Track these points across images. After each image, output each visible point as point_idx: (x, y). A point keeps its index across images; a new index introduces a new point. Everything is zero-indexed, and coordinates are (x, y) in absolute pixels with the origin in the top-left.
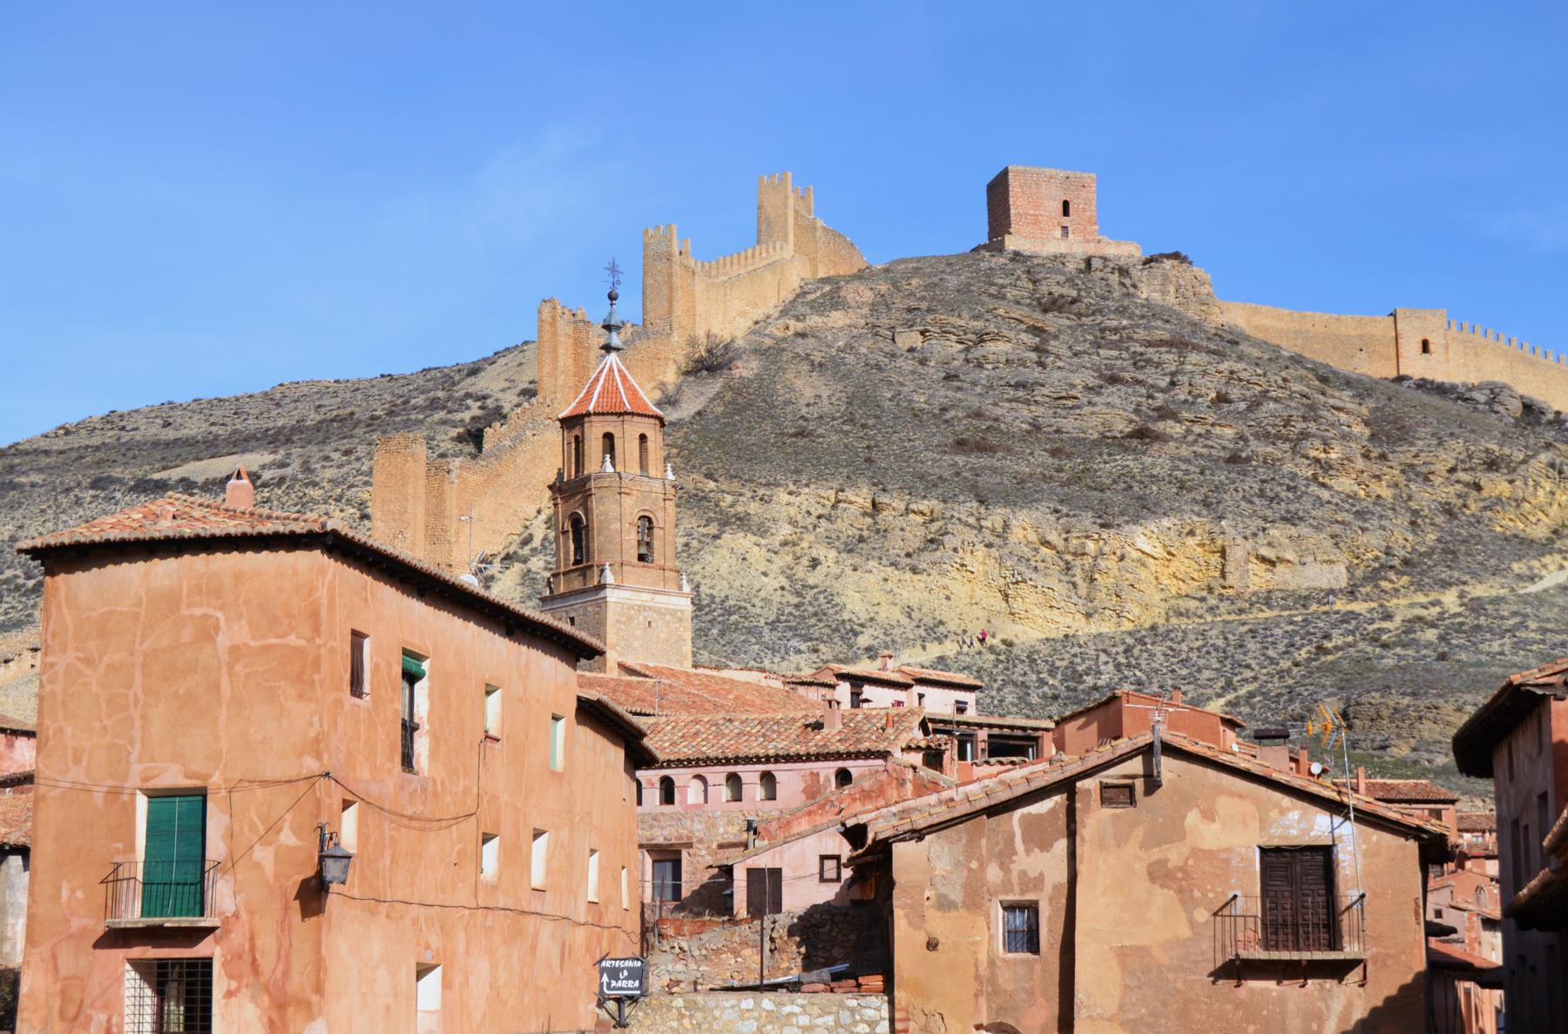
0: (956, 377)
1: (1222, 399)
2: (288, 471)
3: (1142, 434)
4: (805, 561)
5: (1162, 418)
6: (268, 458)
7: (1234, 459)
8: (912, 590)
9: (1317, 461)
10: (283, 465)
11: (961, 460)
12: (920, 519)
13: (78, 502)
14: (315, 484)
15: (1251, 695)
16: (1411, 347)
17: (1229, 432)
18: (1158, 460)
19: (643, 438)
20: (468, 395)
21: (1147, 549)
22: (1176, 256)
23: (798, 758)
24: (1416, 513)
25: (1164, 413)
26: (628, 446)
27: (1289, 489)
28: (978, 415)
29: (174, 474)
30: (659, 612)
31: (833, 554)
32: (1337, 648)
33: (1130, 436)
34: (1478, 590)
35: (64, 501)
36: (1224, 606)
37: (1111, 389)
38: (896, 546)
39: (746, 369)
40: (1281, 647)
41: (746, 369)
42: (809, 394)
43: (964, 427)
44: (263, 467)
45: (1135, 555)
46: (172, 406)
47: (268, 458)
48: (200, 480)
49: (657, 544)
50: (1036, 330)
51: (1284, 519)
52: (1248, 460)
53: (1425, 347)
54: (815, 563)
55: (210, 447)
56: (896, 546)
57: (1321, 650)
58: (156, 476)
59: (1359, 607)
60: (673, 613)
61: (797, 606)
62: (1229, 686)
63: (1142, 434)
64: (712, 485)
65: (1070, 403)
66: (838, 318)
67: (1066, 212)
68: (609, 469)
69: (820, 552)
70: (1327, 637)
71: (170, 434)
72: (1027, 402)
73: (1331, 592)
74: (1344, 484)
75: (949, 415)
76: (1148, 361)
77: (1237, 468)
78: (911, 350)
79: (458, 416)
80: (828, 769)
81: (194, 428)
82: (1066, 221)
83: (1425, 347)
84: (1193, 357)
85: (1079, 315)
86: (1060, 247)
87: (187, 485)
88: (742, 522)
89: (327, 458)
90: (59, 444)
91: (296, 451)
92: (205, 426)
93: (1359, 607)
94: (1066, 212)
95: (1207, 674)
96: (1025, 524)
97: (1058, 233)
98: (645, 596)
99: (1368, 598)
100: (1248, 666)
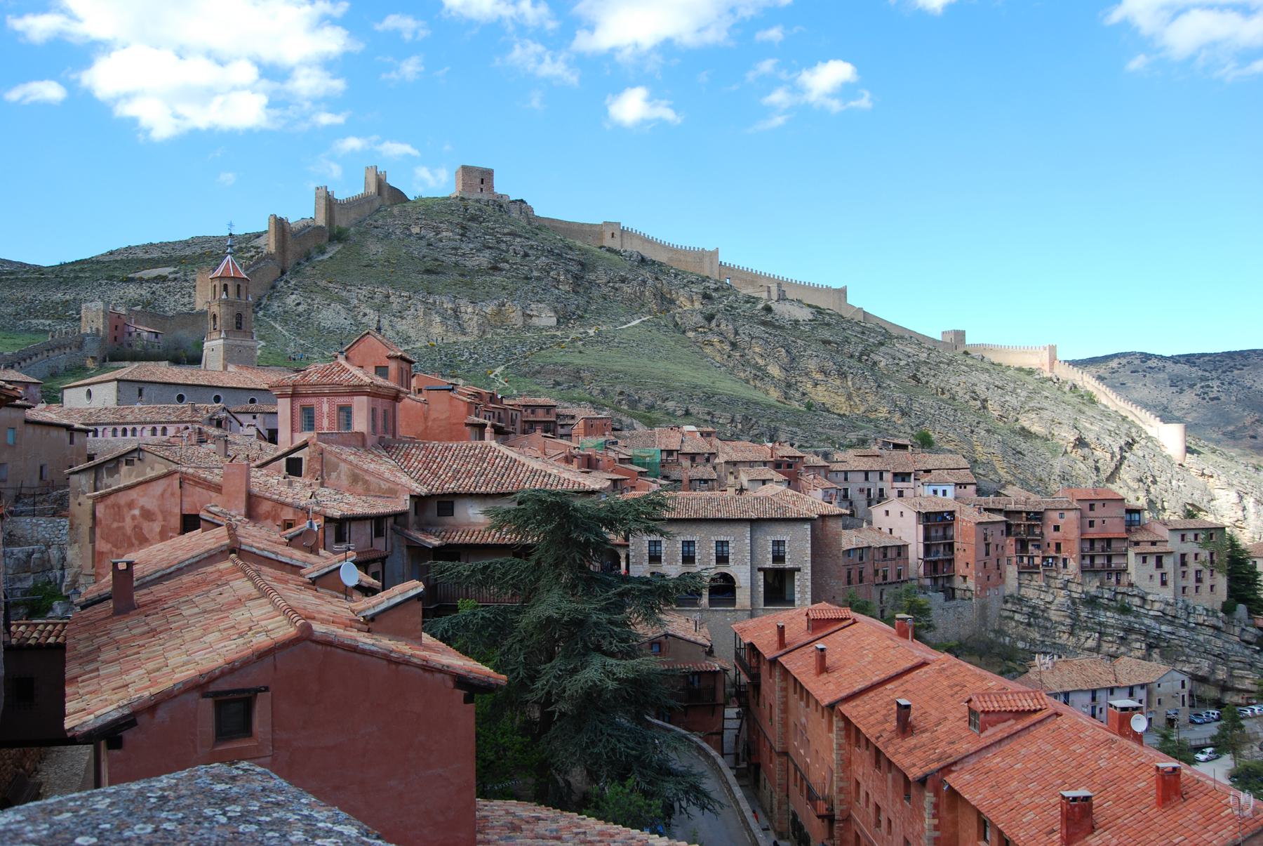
0: (431, 245)
1: (526, 255)
2: (178, 275)
3: (495, 268)
4: (361, 313)
5: (504, 262)
6: (172, 269)
7: (526, 278)
9: (556, 279)
10: (177, 273)
11: (425, 277)
12: (405, 299)
13: (100, 285)
14: (186, 281)
15: (513, 365)
16: (608, 236)
17: (526, 268)
18: (498, 279)
19: (239, 286)
20: (252, 247)
21: (487, 311)
22: (522, 201)
23: (172, 422)
24: (591, 298)
26: (231, 289)
27: (543, 290)
28: (436, 260)
29: (138, 275)
30: (245, 347)
31: (372, 311)
32: (547, 348)
33: (491, 269)
34: (604, 328)
35: (95, 284)
36: (513, 332)
37: (487, 251)
38: (395, 307)
40: (528, 347)
42: (374, 251)
43: (429, 264)
44: (170, 273)
45: (482, 313)
46: (151, 244)
47: (172, 269)
48: (146, 278)
49: (243, 323)
50: (463, 228)
51: (537, 301)
52: (531, 278)
54: (365, 315)
55: (155, 263)
56: (395, 307)
57: (541, 348)
58: (130, 276)
59: (559, 333)
60: (249, 347)
61: (355, 331)
62: (508, 361)
64: (331, 285)
65: (471, 256)
67: (482, 183)
68: (224, 296)
69: (368, 311)
70: (545, 344)
71: (147, 256)
72: (455, 255)
73: (551, 327)
75: (425, 259)
76: (502, 241)
77: (525, 281)
78: (417, 234)
79: (245, 255)
80: (182, 426)
81: (156, 254)
82: (482, 186)
83: (613, 234)
84: (518, 240)
85: (481, 223)
86: (480, 196)
87: (141, 280)
89: (193, 271)
90: (107, 259)
91: (183, 267)
92: (160, 254)
93: (559, 333)
94: (482, 183)
95: (500, 356)
97: (479, 190)
98: (239, 342)
99: (563, 330)
100: (515, 354)
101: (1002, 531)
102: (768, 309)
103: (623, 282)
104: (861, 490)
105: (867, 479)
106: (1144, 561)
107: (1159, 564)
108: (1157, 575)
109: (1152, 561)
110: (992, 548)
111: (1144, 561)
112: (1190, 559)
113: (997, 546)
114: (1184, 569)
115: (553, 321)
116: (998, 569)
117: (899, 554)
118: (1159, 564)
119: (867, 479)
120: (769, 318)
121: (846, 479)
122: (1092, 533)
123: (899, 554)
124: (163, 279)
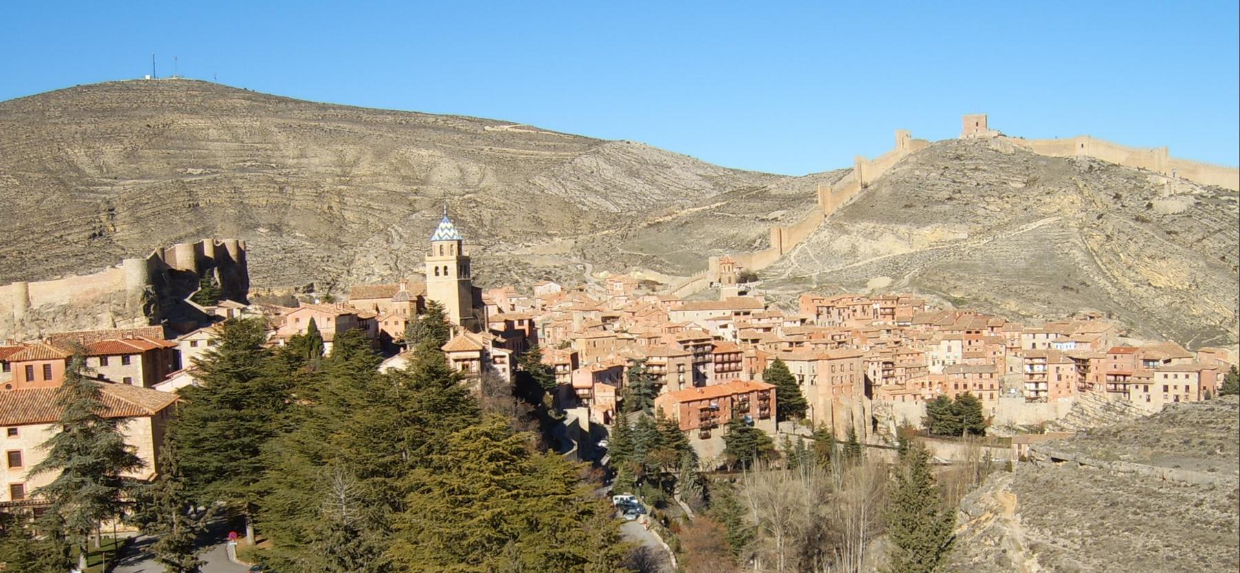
1: (978, 184)
3: (950, 199)
8: (875, 245)
11: (904, 210)
25: (960, 192)
39: (871, 188)
41: (871, 188)
53: (1082, 145)
63: (950, 199)
66: (905, 167)
67: (977, 125)
74: (991, 207)
83: (1082, 145)
88: (847, 232)
94: (977, 125)
96: (903, 229)
101: (1072, 369)
102: (1150, 206)
103: (1048, 193)
104: (1044, 344)
105: (1048, 337)
106: (1137, 387)
107: (1146, 389)
108: (1145, 395)
109: (1141, 387)
110: (1063, 377)
111: (1137, 387)
112: (1171, 389)
113: (1067, 377)
114: (1166, 393)
115: (965, 236)
116: (1068, 387)
117: (991, 377)
118: (1146, 389)
119: (1048, 337)
120: (1144, 213)
121: (1034, 338)
122: (1115, 371)
123: (991, 377)
124: (776, 219)
